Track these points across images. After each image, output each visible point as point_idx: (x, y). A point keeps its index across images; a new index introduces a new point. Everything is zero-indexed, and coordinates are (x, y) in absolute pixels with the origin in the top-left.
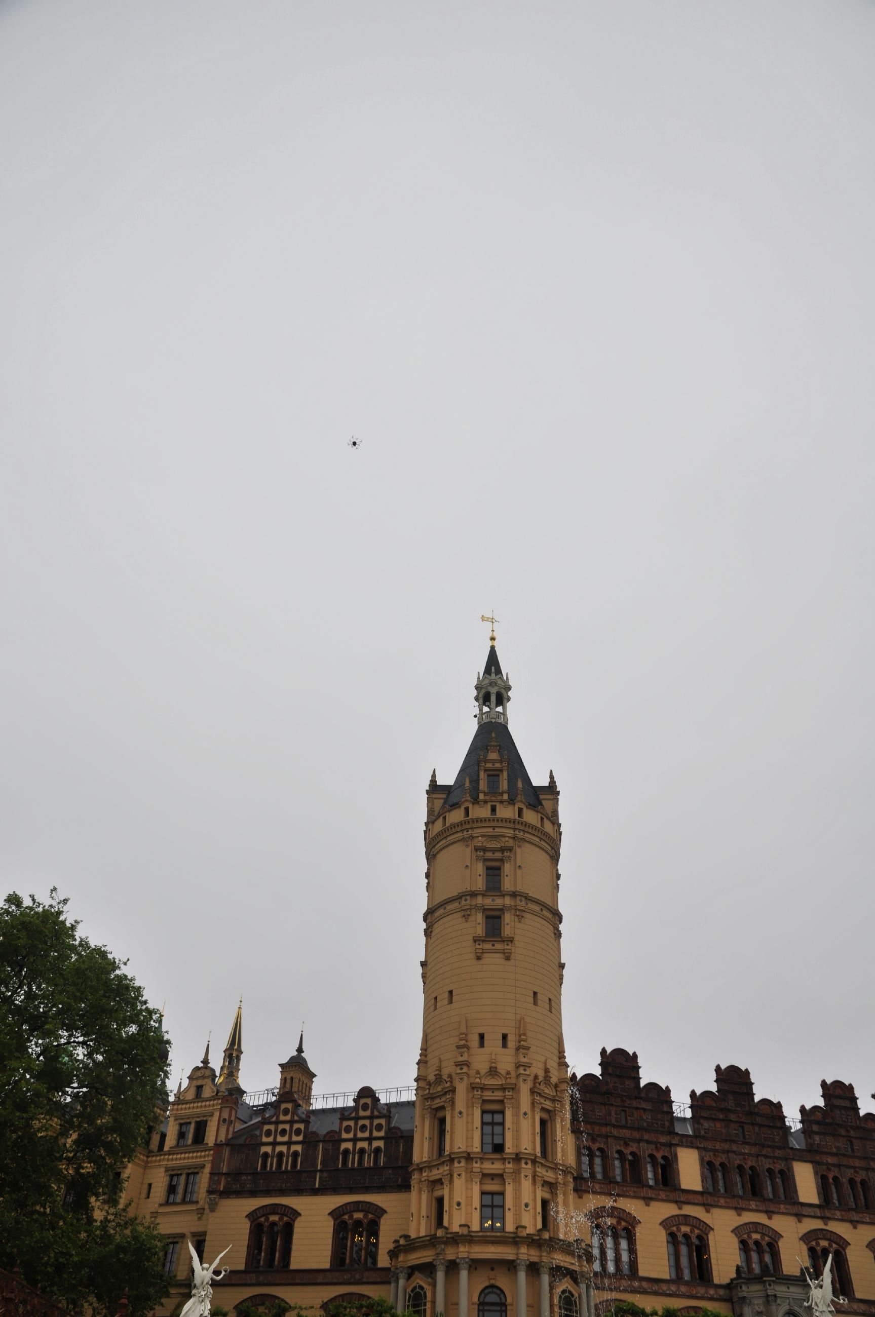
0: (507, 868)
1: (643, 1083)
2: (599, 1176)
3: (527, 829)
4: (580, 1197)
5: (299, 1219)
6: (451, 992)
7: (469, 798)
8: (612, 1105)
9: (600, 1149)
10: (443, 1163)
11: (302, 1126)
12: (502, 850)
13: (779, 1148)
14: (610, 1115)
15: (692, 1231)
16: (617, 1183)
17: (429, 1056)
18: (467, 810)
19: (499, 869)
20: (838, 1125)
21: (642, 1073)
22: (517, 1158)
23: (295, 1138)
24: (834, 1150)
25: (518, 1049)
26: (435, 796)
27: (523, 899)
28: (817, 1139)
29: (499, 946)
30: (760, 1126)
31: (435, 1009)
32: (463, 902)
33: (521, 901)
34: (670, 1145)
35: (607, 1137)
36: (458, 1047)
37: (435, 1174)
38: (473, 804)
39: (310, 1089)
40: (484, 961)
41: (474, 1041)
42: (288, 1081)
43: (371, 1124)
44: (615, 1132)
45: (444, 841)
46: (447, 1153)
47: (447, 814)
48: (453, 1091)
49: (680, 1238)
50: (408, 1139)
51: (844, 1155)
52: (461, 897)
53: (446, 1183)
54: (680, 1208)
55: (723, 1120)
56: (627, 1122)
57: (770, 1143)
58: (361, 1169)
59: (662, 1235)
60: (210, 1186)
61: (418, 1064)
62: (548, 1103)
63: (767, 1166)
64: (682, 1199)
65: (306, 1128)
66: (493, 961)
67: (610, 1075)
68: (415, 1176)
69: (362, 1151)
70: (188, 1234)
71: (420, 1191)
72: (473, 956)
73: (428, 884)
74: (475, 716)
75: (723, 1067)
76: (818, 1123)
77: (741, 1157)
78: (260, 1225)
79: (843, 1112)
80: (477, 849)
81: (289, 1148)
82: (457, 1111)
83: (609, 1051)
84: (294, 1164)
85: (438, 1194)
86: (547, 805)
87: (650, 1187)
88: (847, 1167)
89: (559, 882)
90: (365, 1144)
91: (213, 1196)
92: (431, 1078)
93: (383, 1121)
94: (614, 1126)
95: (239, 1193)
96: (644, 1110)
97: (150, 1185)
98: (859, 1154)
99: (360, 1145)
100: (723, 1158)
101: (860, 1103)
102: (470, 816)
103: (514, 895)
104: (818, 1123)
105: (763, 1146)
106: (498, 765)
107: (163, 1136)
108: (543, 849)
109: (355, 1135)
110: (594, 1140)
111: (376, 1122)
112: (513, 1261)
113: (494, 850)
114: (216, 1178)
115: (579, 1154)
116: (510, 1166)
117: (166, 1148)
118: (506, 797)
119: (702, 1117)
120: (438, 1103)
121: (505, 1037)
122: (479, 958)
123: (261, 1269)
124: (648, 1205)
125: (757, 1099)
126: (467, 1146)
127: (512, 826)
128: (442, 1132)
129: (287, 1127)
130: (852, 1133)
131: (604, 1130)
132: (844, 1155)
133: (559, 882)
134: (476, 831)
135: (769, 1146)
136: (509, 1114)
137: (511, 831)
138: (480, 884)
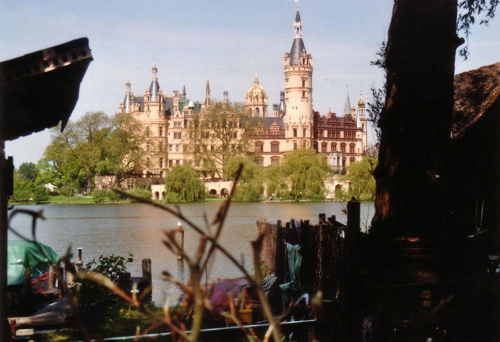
18: (299, 68)
22: (308, 138)
29: (305, 99)
48: (298, 126)
66: (305, 102)
80: (301, 78)
93: (278, 126)
103: (308, 88)
106: (305, 57)
113: (304, 78)
121: (306, 116)
122: (302, 101)
138: (301, 86)
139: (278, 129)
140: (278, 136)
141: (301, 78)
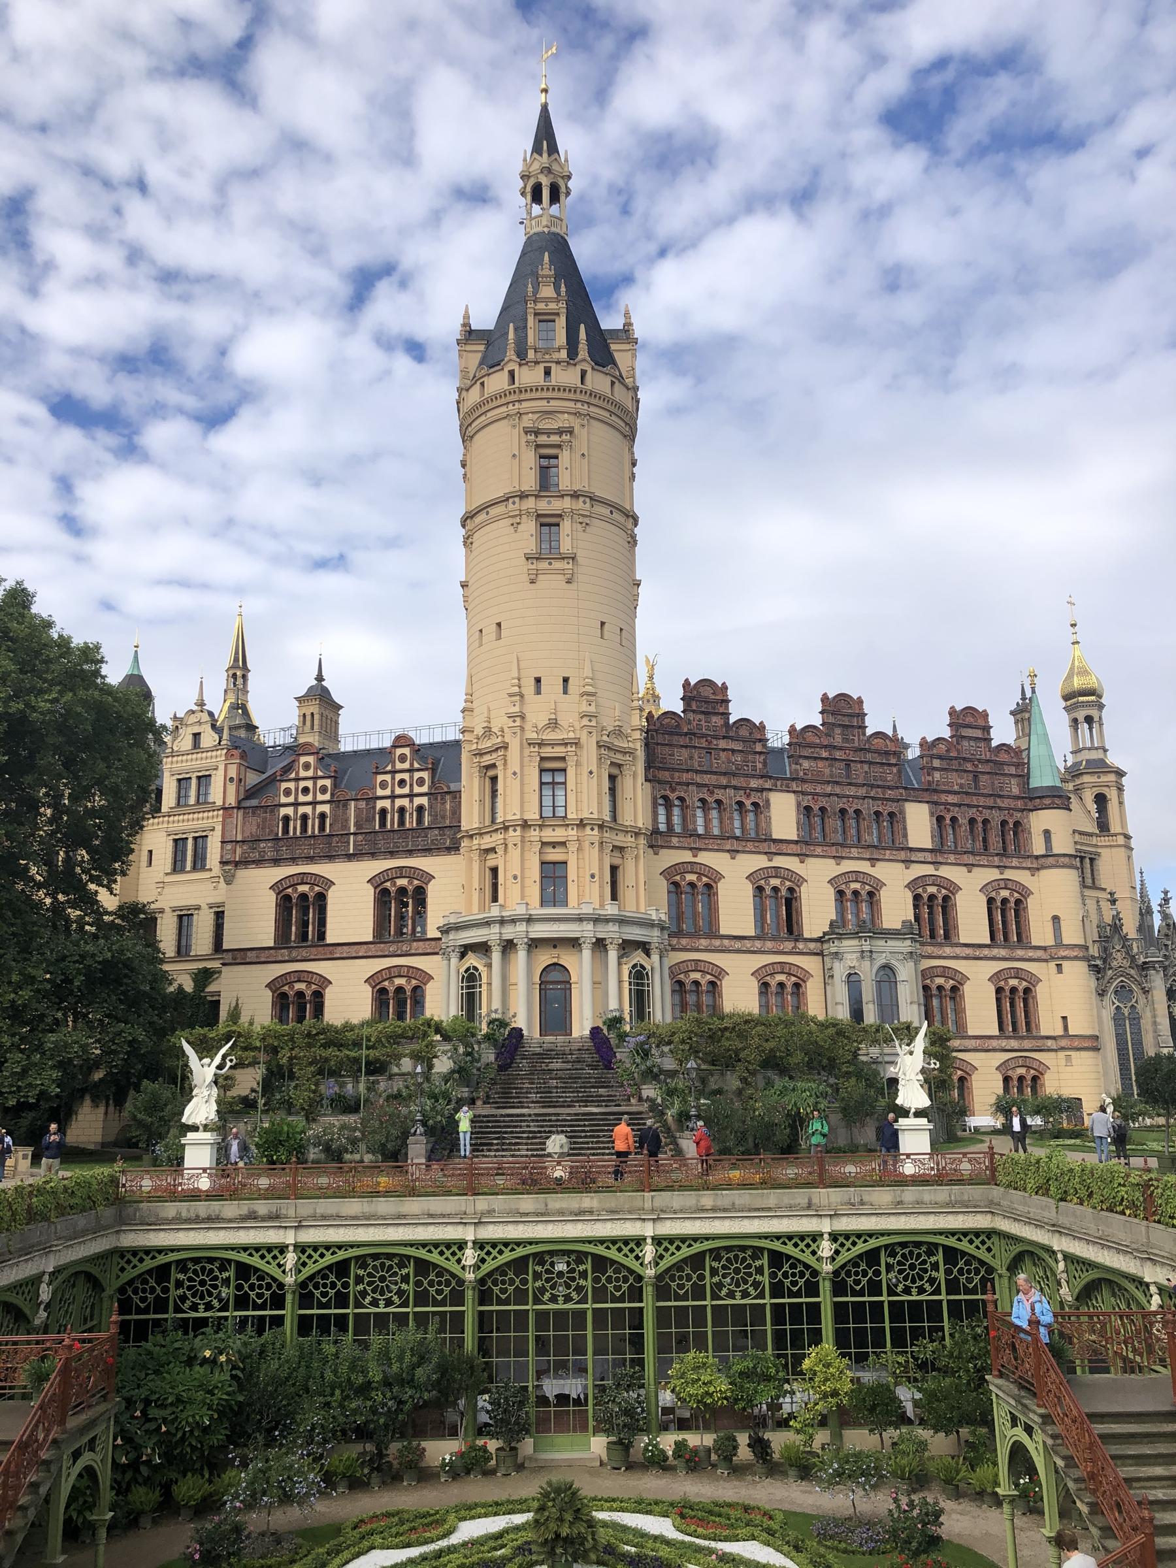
0: (565, 457)
1: (732, 719)
2: (678, 829)
3: (593, 401)
4: (656, 854)
5: (333, 888)
6: (499, 625)
7: (514, 357)
8: (695, 747)
9: (681, 799)
10: (497, 830)
11: (328, 783)
12: (560, 432)
13: (889, 788)
14: (691, 758)
15: (782, 884)
16: (699, 836)
17: (475, 705)
18: (512, 374)
19: (557, 457)
20: (964, 759)
21: (732, 708)
22: (581, 824)
23: (320, 797)
24: (956, 788)
25: (582, 695)
26: (469, 348)
27: (588, 500)
28: (937, 775)
29: (557, 565)
30: (870, 763)
31: (481, 645)
32: (511, 506)
33: (585, 502)
34: (762, 790)
35: (688, 784)
36: (511, 695)
37: (487, 842)
38: (520, 365)
39: (337, 723)
40: (539, 584)
41: (529, 688)
42: (308, 718)
43: (411, 778)
44: (698, 779)
45: (483, 418)
46: (499, 820)
47: (485, 379)
48: (506, 748)
49: (768, 891)
50: (456, 795)
51: (967, 793)
52: (507, 499)
53: (500, 851)
54: (770, 860)
55: (827, 759)
56: (711, 766)
57: (880, 783)
58: (402, 831)
59: (749, 889)
60: (222, 857)
61: (463, 712)
62: (619, 756)
63: (876, 809)
64: (773, 850)
65: (335, 785)
66: (551, 583)
67: (694, 711)
68: (465, 843)
69: (402, 810)
70: (204, 906)
71: (471, 860)
72: (526, 578)
73: (465, 475)
74: (522, 223)
75: (831, 696)
76: (940, 757)
77: (845, 800)
78: (288, 898)
79: (972, 743)
80: (527, 431)
81: (314, 809)
82: (509, 772)
83: (693, 683)
84: (322, 827)
85: (491, 863)
86: (622, 359)
87: (737, 838)
88: (969, 806)
89: (635, 470)
90: (405, 802)
91: (227, 868)
92: (479, 731)
93: (425, 775)
94: (697, 772)
95: (258, 863)
96: (733, 751)
97: (150, 852)
98: (985, 791)
99: (399, 802)
100: (823, 802)
101: (993, 733)
102: (517, 385)
103: (575, 495)
104: (940, 757)
105: (872, 786)
106: (552, 306)
107: (159, 792)
108: (614, 427)
109: (393, 791)
110: (673, 790)
111: (417, 775)
112: (578, 939)
113: (549, 433)
114: (229, 847)
115: (655, 805)
116: (572, 833)
117: (164, 809)
118: (563, 354)
119: (801, 757)
120: (487, 760)
121: (566, 680)
123: (293, 944)
124: (733, 858)
125: (869, 732)
126: (522, 811)
127: (572, 396)
128: (494, 792)
129: (309, 784)
130: (981, 768)
131: (685, 777)
132: (967, 793)
133: (635, 470)
134: (525, 404)
135: (878, 787)
136: (571, 772)
137: (572, 404)
138: (530, 482)
139: (425, 789)
140: (420, 829)
141: (527, 431)
